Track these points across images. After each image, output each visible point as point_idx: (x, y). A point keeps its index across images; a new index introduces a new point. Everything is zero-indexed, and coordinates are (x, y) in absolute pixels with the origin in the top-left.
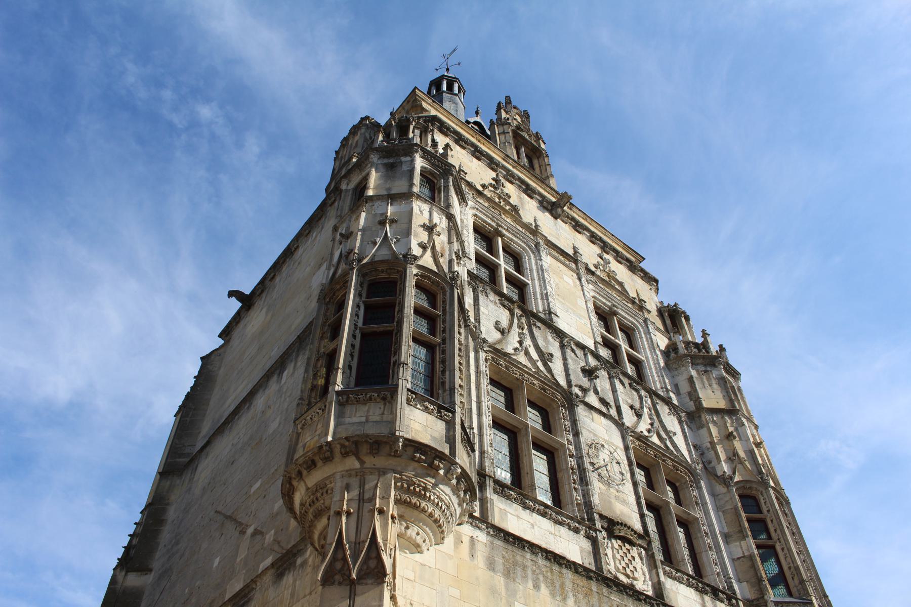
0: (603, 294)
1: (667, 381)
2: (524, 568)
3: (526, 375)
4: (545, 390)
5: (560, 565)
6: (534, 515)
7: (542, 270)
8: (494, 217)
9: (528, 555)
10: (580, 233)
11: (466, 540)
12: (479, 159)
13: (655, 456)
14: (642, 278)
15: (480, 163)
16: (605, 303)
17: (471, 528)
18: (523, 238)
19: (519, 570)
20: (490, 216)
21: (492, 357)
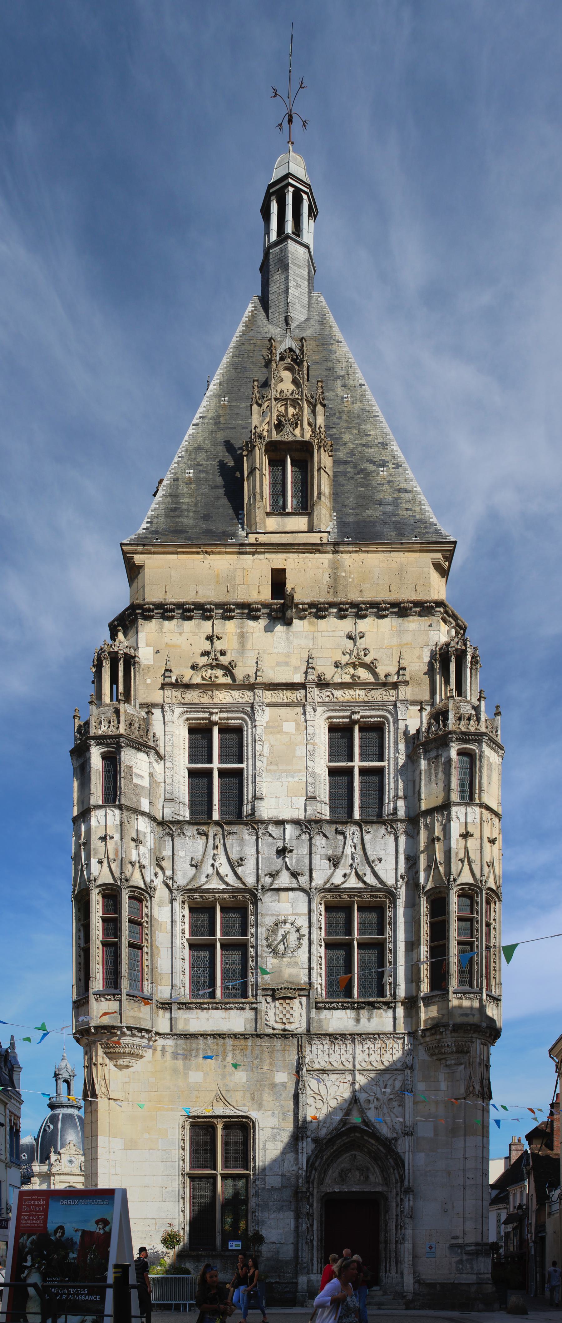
0: (338, 708)
1: (401, 784)
2: (198, 1050)
3: (217, 895)
4: (234, 897)
5: (224, 1038)
6: (210, 1011)
7: (255, 741)
8: (203, 708)
9: (201, 1041)
10: (324, 617)
11: (159, 1048)
12: (190, 618)
13: (350, 897)
14: (420, 615)
15: (193, 622)
16: (341, 716)
17: (163, 1040)
18: (237, 708)
19: (194, 1053)
20: (200, 709)
21: (189, 897)
